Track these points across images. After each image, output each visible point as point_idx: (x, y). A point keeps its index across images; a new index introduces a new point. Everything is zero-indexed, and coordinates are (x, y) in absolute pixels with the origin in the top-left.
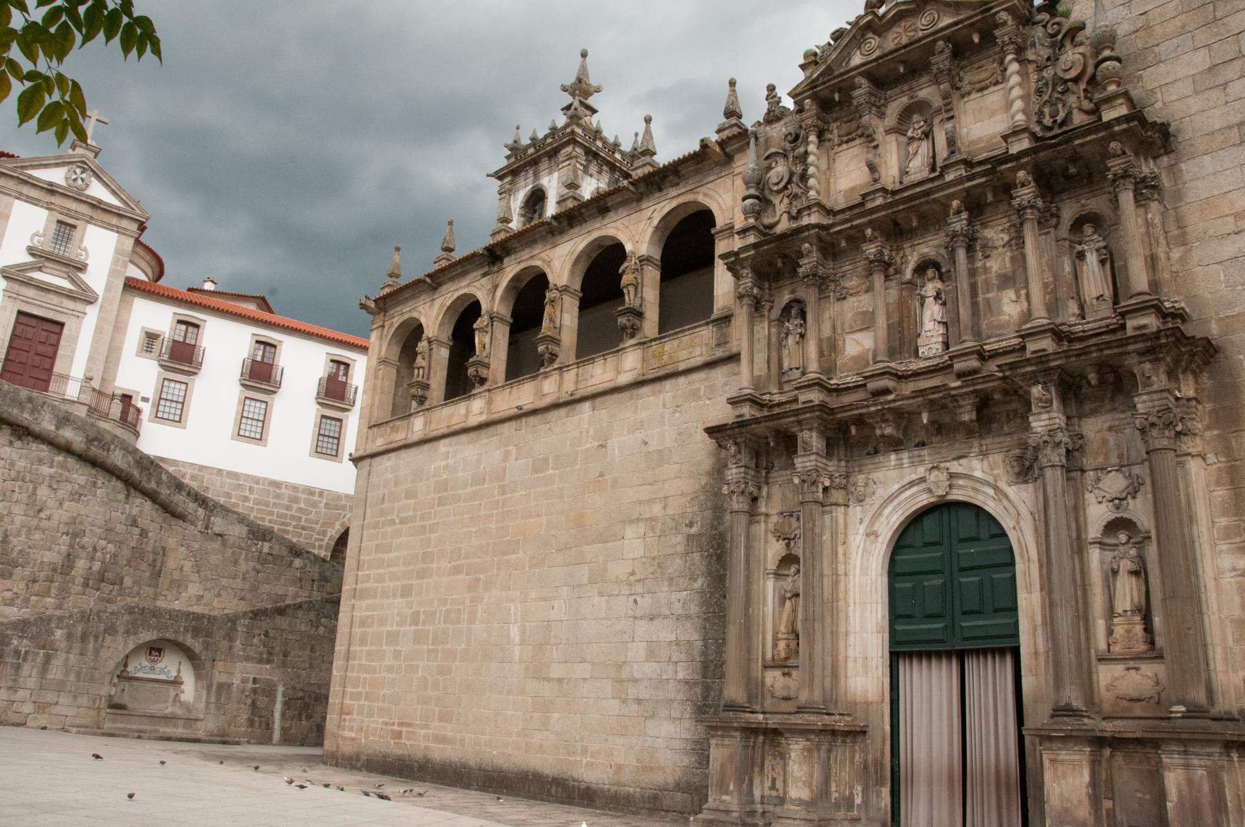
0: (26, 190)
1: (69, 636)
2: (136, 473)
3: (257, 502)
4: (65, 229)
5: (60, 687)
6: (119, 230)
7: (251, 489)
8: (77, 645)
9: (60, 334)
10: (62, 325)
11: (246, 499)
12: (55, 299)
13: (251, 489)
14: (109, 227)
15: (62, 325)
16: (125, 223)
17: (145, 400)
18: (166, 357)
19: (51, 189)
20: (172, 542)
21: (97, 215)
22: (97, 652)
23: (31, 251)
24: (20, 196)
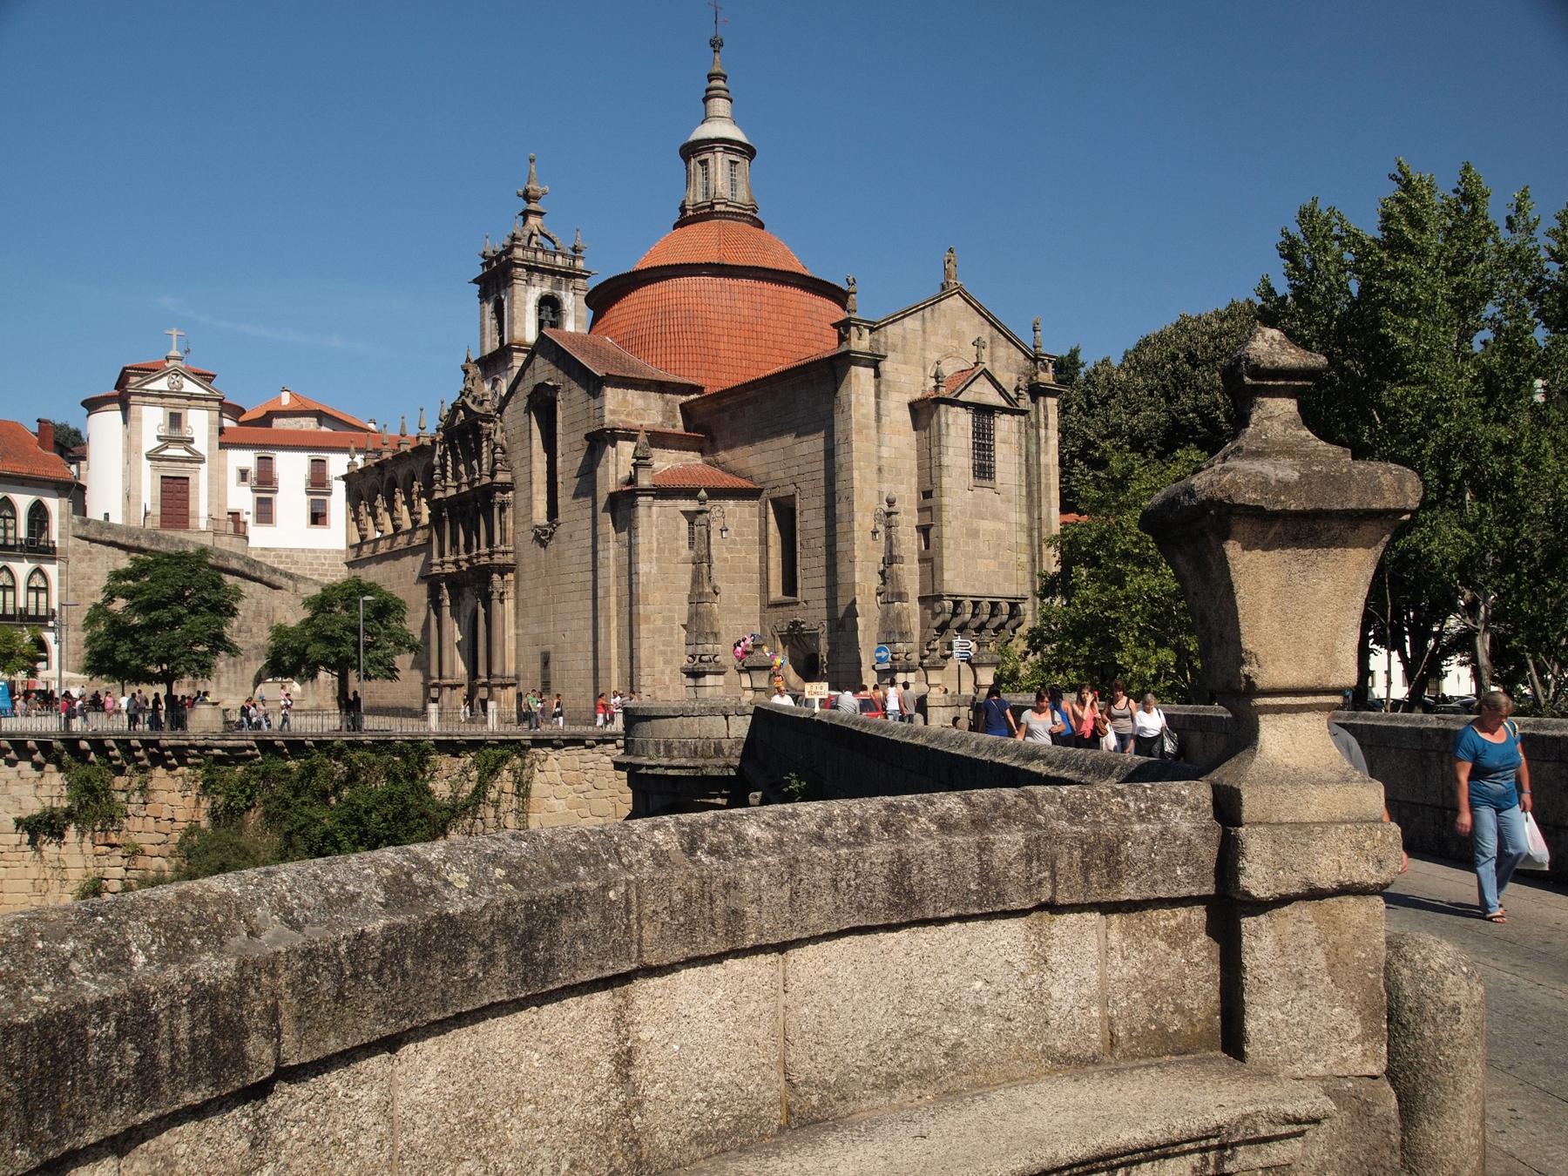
0: (147, 399)
1: (227, 665)
2: (247, 570)
3: (330, 565)
4: (175, 420)
5: (228, 690)
6: (207, 408)
7: (325, 558)
8: (232, 669)
9: (187, 484)
10: (187, 478)
11: (324, 564)
12: (180, 464)
13: (325, 558)
14: (201, 408)
15: (187, 478)
16: (210, 404)
17: (248, 513)
18: (255, 484)
19: (161, 394)
20: (277, 603)
21: (193, 402)
22: (242, 670)
23: (159, 438)
24: (144, 404)
